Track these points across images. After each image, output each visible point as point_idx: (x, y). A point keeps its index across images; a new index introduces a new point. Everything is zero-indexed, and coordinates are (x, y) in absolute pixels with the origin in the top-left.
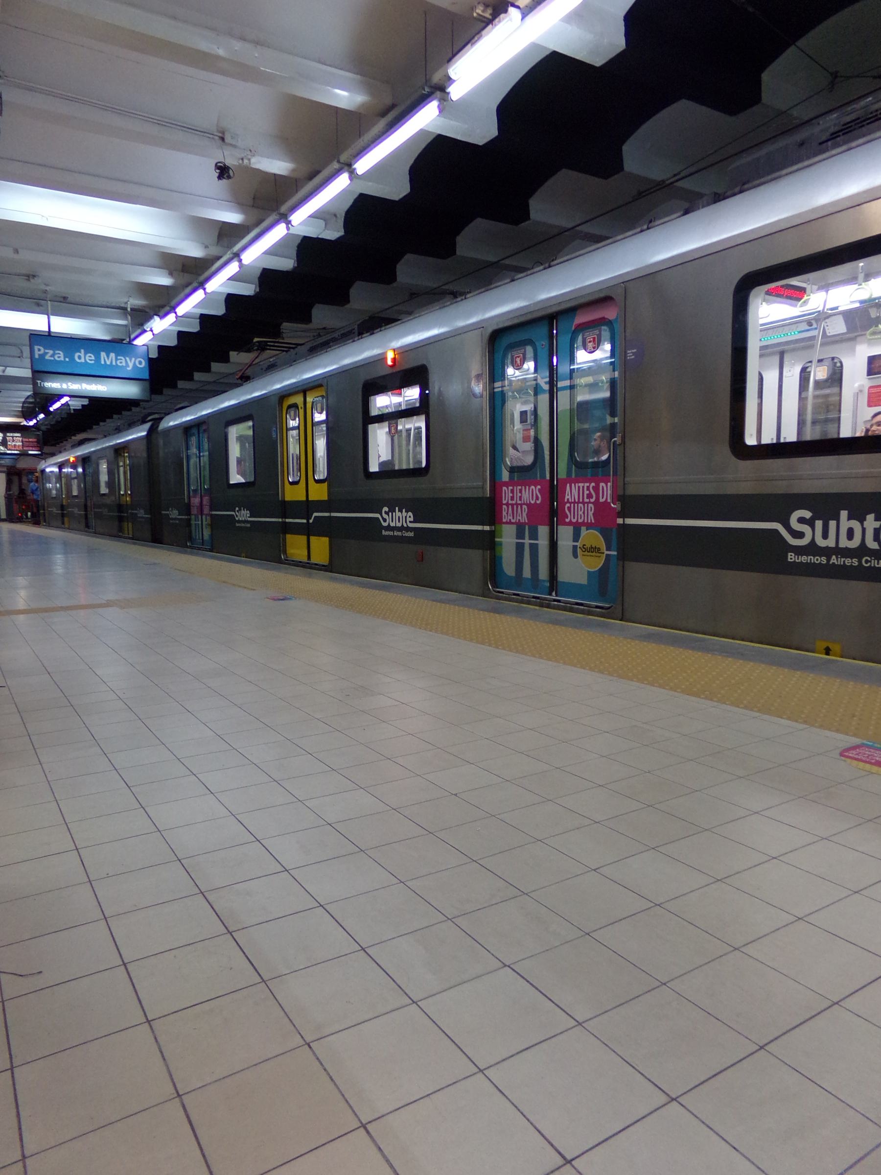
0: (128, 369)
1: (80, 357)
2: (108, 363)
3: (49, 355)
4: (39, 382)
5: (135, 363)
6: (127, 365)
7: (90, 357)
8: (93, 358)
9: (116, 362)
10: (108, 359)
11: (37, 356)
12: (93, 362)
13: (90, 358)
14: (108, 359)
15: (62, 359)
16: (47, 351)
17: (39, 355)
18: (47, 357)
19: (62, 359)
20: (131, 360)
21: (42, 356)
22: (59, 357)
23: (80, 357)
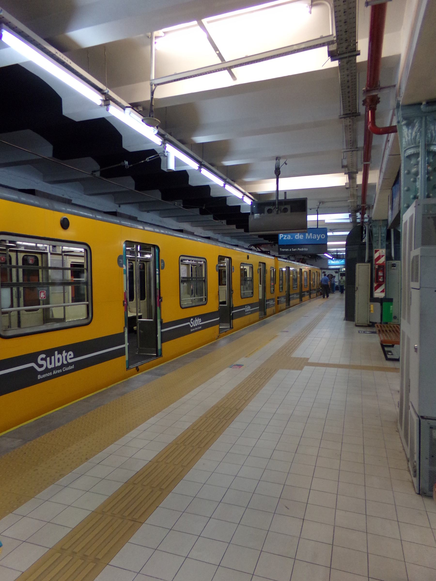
0: (318, 240)
1: (297, 237)
3: (285, 237)
4: (281, 249)
5: (320, 237)
6: (317, 238)
8: (303, 236)
9: (312, 237)
10: (309, 236)
11: (280, 239)
12: (302, 238)
14: (309, 236)
15: (290, 238)
16: (284, 236)
17: (281, 238)
18: (284, 238)
19: (290, 238)
20: (319, 236)
21: (282, 238)
22: (289, 238)
23: (297, 237)
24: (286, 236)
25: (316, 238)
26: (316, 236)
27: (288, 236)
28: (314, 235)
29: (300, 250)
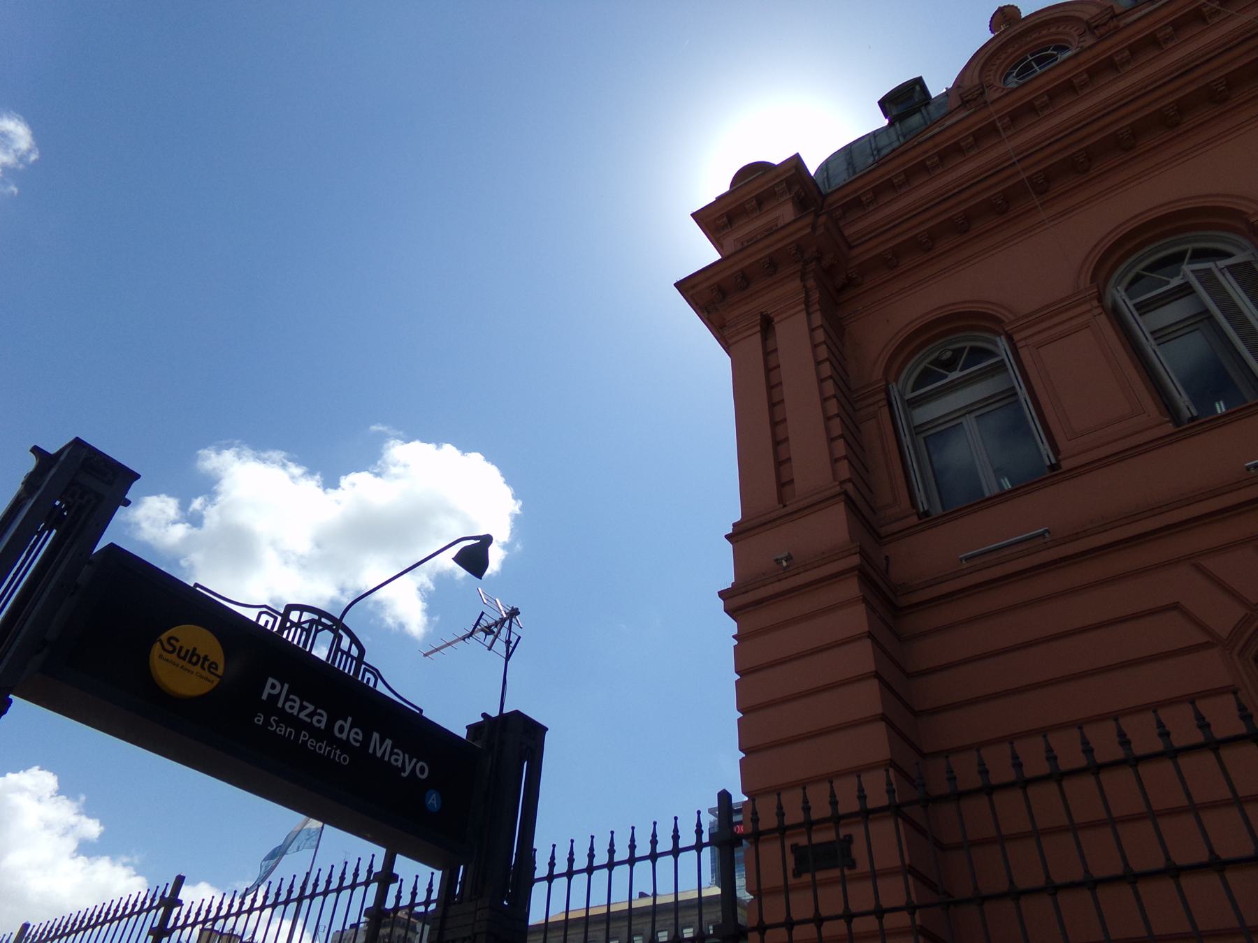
1: (341, 729)
2: (379, 754)
8: (360, 738)
13: (355, 736)
23: (341, 729)
24: (311, 708)
25: (399, 764)
27: (319, 711)
29: (311, 743)
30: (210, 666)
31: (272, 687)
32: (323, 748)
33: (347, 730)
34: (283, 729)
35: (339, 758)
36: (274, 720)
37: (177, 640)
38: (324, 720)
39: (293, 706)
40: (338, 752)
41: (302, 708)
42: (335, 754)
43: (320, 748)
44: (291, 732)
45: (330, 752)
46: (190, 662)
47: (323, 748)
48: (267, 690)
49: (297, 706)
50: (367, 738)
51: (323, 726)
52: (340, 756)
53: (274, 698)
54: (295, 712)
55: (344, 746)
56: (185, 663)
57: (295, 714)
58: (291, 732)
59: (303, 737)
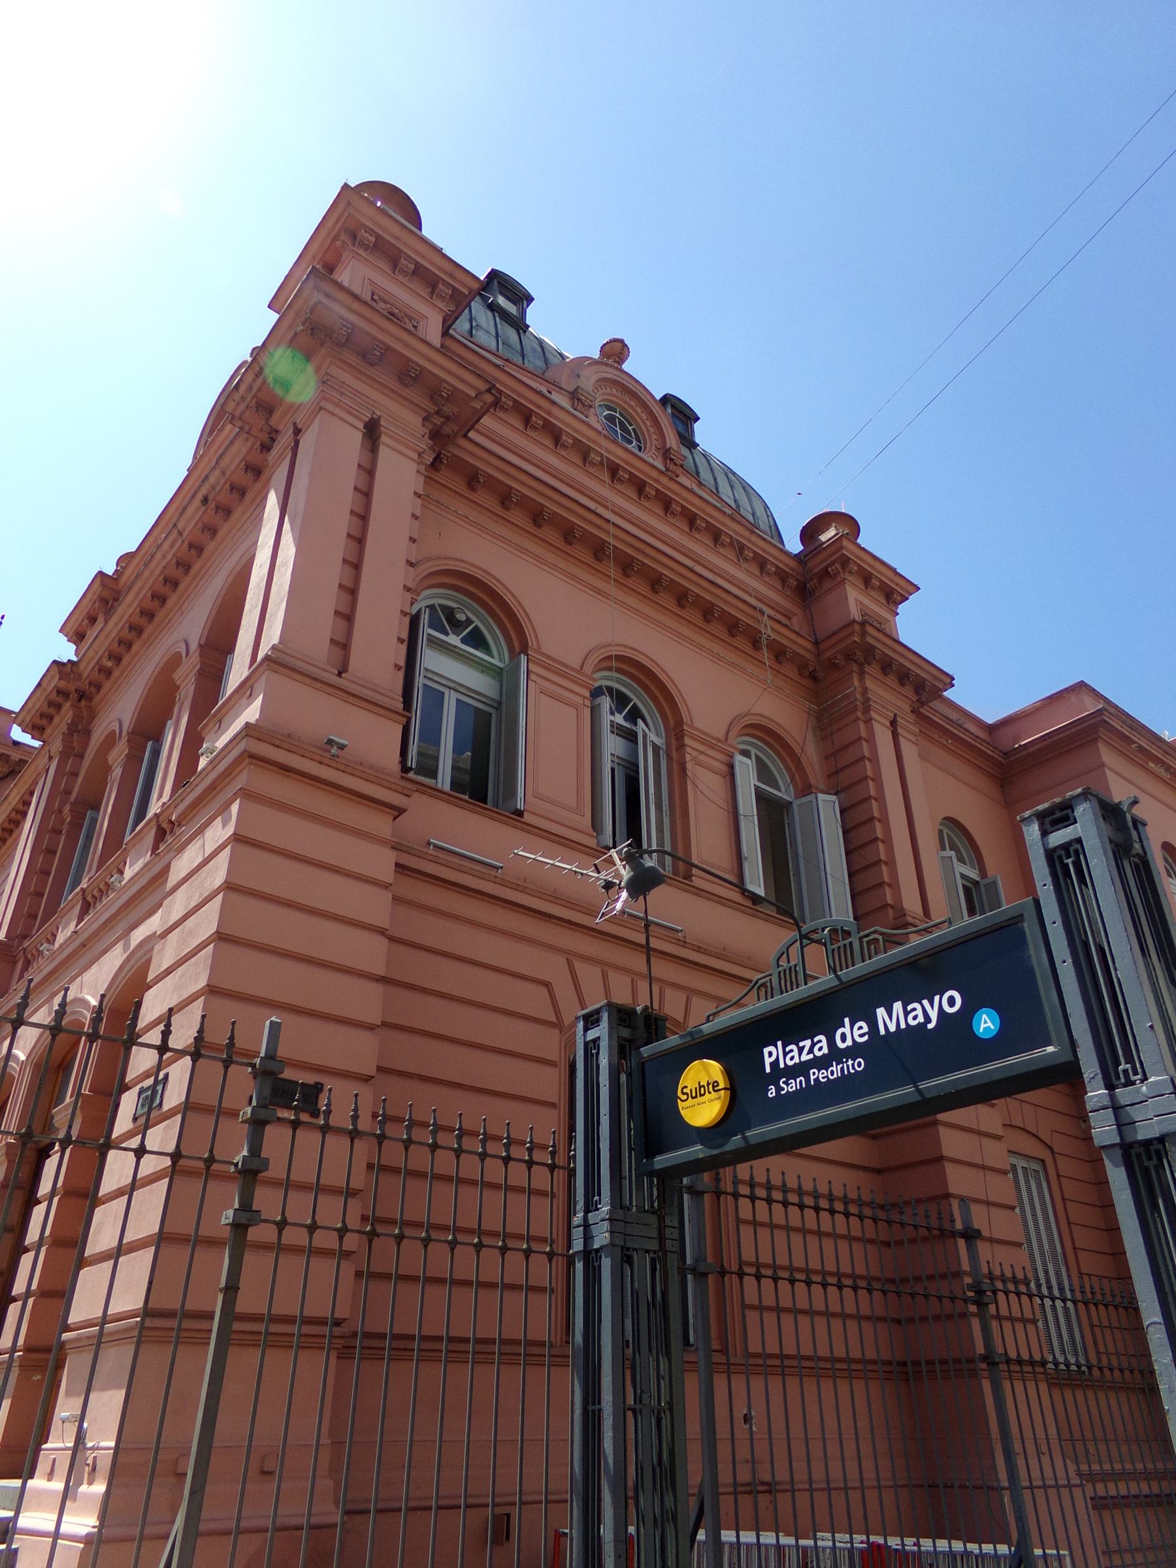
2: (892, 1028)
6: (928, 1019)
7: (860, 1028)
8: (866, 1029)
12: (866, 1038)
25: (921, 1019)
26: (919, 1012)
27: (816, 1039)
28: (909, 1008)
30: (713, 1087)
31: (771, 1054)
32: (835, 1071)
33: (852, 1033)
34: (794, 1084)
35: (853, 1068)
36: (784, 1083)
37: (686, 1087)
38: (824, 1044)
39: (795, 1056)
40: (850, 1062)
41: (801, 1050)
42: (848, 1066)
43: (832, 1073)
44: (801, 1081)
45: (842, 1069)
46: (701, 1095)
47: (835, 1071)
48: (768, 1061)
49: (796, 1053)
50: (873, 1024)
51: (825, 1050)
52: (853, 1065)
53: (775, 1064)
54: (796, 1060)
55: (855, 1051)
56: (699, 1099)
57: (798, 1061)
58: (801, 1081)
59: (814, 1074)
